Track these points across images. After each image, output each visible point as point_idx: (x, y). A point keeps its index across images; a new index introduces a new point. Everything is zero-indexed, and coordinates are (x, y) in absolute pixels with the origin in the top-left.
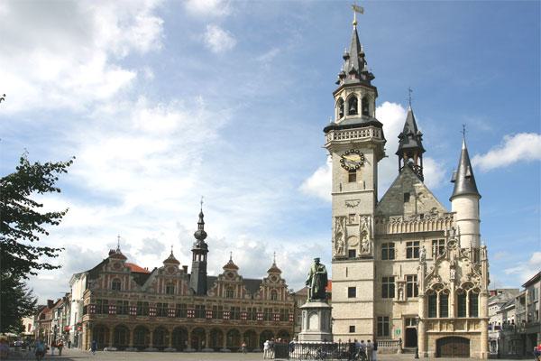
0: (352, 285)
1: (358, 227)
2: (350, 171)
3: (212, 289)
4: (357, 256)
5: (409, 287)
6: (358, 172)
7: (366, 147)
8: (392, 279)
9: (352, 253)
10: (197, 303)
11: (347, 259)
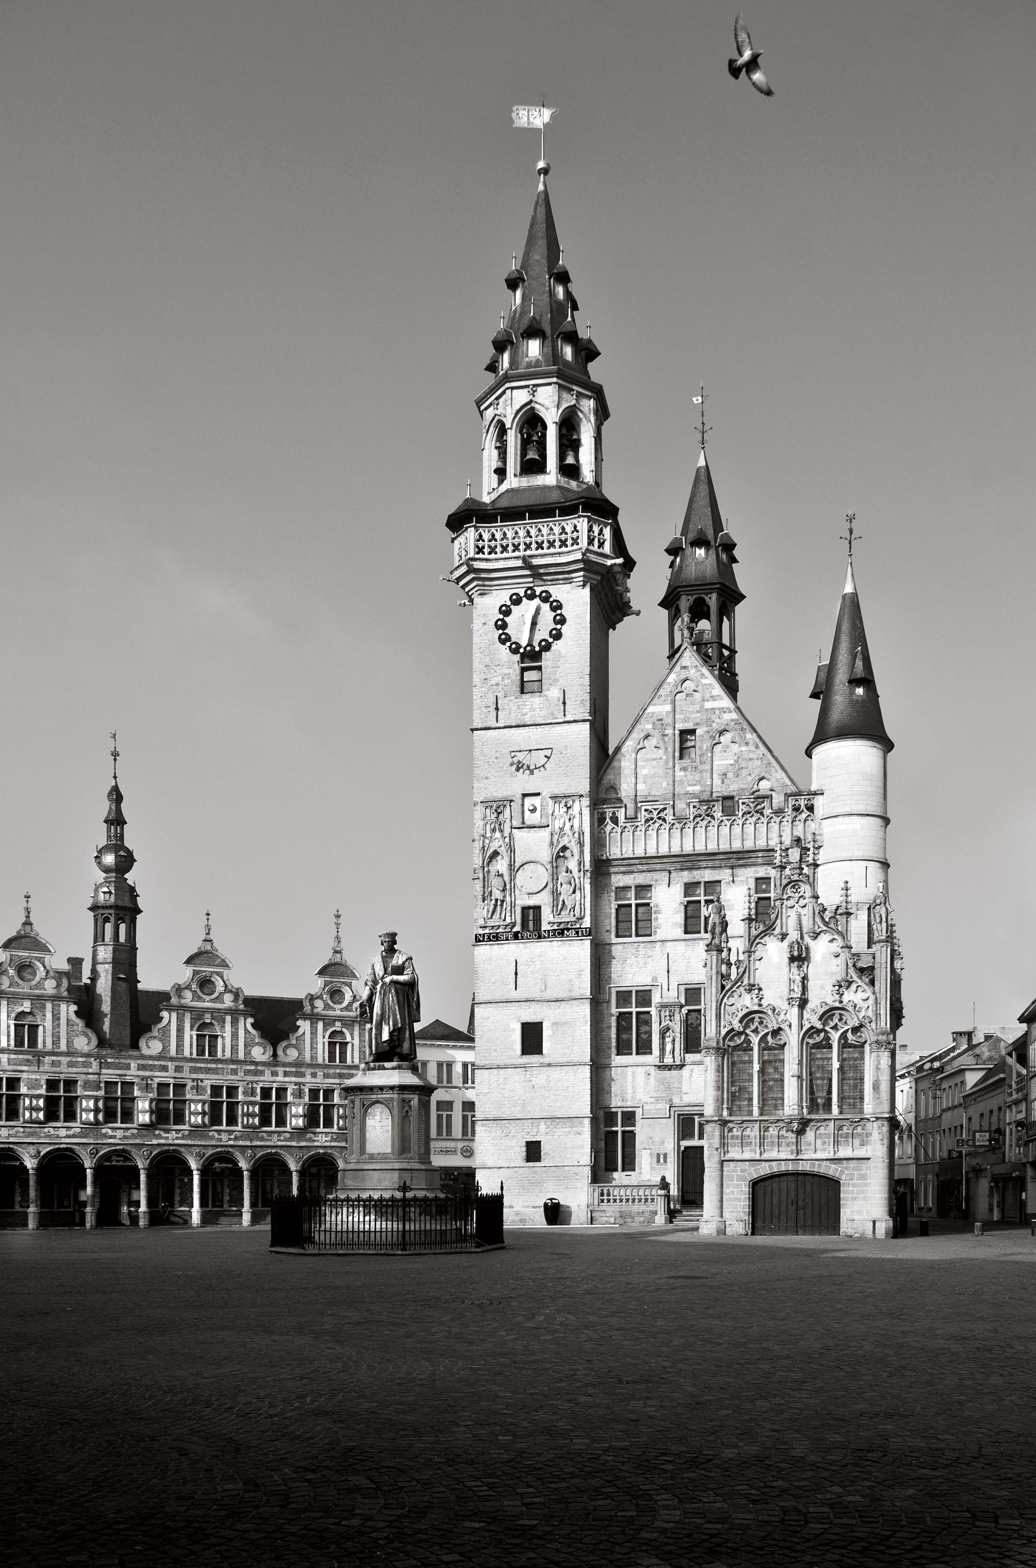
1: (545, 834)
3: (155, 1033)
8: (644, 997)
10: (109, 1074)
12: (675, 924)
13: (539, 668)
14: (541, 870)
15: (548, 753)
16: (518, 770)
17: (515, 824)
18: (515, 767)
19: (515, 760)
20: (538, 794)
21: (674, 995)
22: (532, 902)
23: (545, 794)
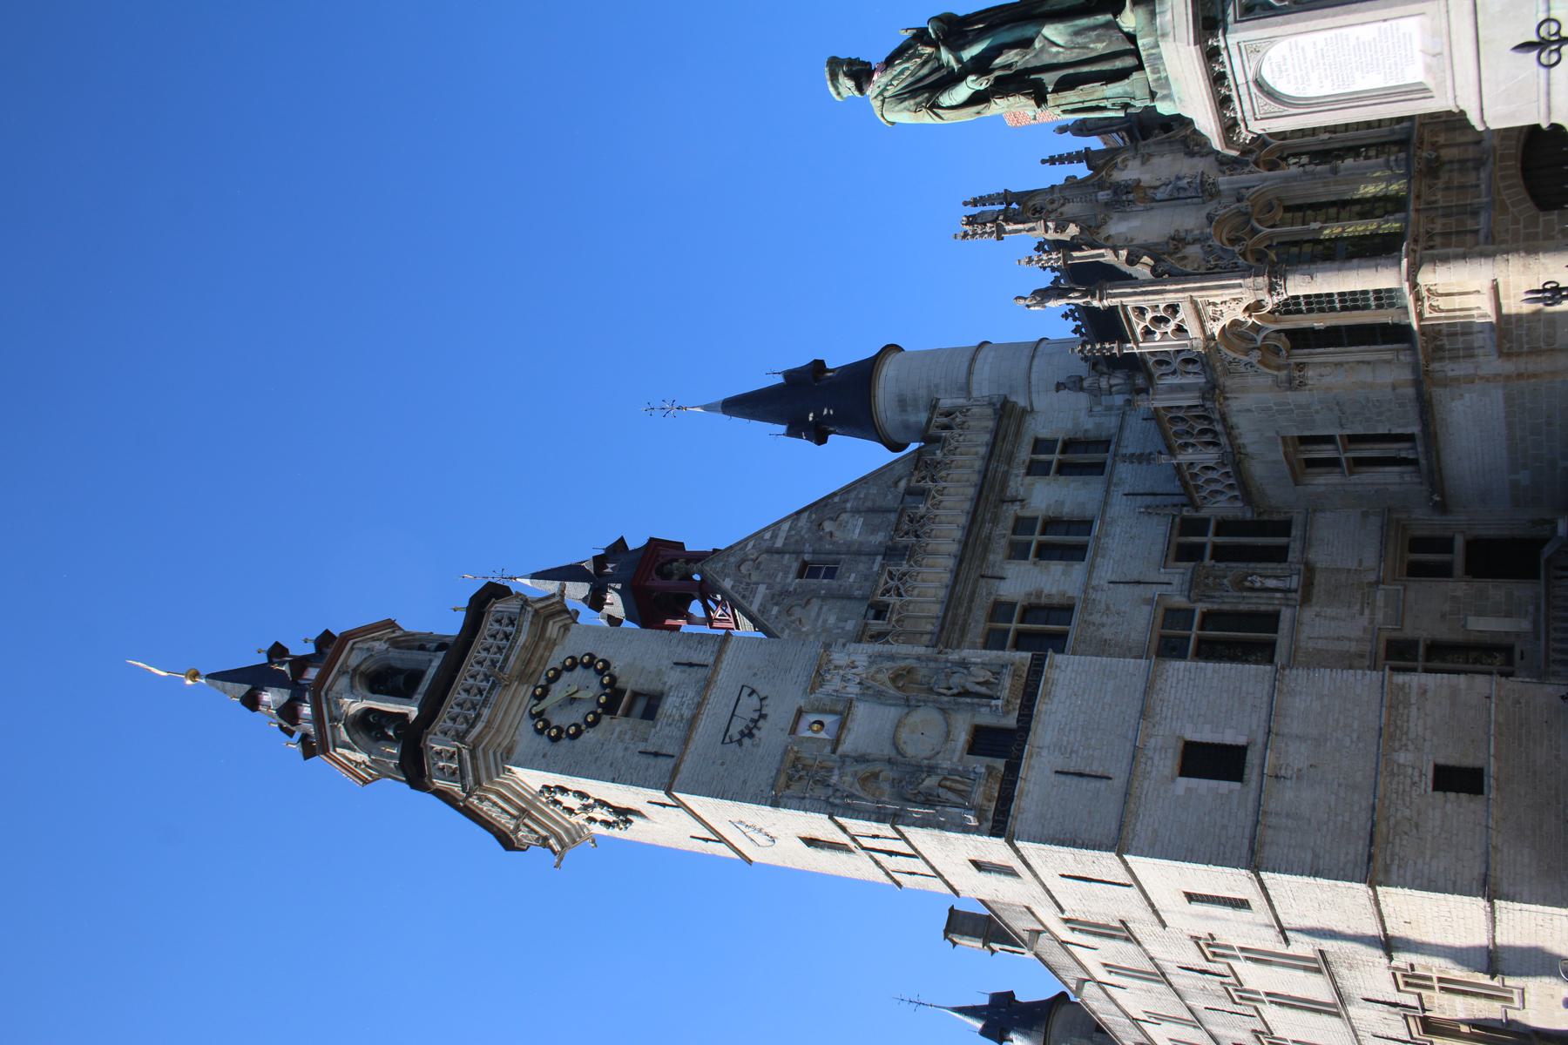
0: (1167, 762)
1: (861, 711)
2: (610, 708)
4: (1011, 721)
5: (1220, 553)
6: (629, 683)
7: (552, 644)
9: (984, 741)
11: (1013, 769)
12: (1064, 573)
13: (636, 695)
14: (918, 716)
15: (746, 691)
16: (751, 735)
17: (828, 749)
18: (746, 741)
19: (737, 737)
20: (800, 713)
21: (1178, 574)
22: (962, 737)
23: (802, 703)
